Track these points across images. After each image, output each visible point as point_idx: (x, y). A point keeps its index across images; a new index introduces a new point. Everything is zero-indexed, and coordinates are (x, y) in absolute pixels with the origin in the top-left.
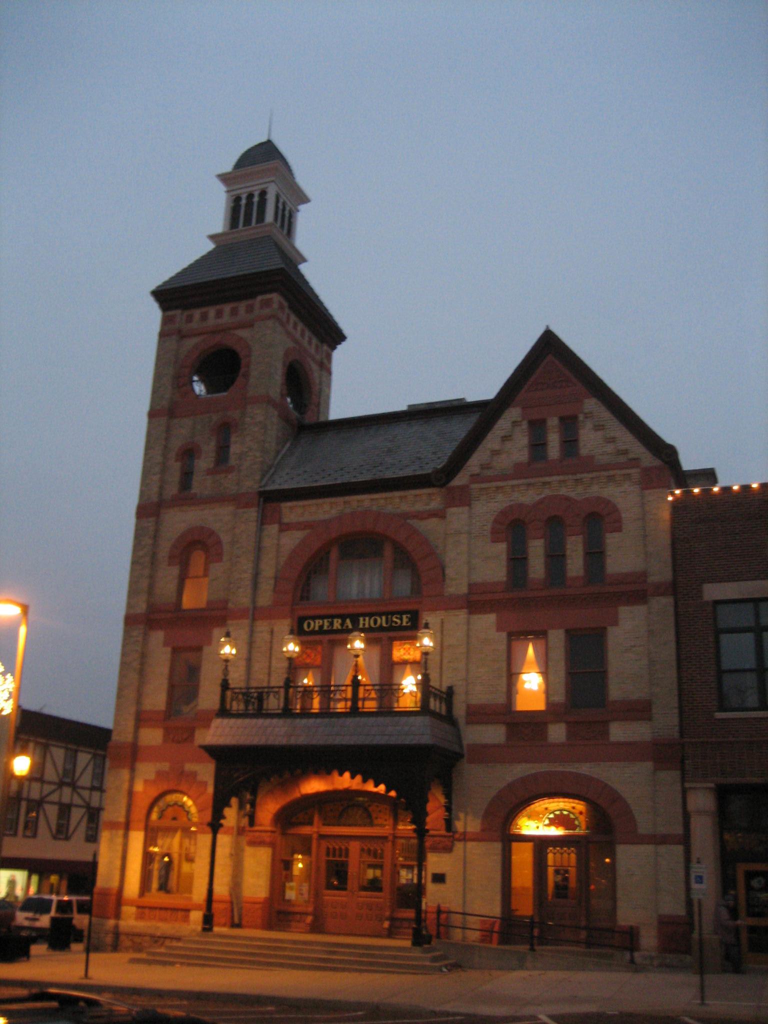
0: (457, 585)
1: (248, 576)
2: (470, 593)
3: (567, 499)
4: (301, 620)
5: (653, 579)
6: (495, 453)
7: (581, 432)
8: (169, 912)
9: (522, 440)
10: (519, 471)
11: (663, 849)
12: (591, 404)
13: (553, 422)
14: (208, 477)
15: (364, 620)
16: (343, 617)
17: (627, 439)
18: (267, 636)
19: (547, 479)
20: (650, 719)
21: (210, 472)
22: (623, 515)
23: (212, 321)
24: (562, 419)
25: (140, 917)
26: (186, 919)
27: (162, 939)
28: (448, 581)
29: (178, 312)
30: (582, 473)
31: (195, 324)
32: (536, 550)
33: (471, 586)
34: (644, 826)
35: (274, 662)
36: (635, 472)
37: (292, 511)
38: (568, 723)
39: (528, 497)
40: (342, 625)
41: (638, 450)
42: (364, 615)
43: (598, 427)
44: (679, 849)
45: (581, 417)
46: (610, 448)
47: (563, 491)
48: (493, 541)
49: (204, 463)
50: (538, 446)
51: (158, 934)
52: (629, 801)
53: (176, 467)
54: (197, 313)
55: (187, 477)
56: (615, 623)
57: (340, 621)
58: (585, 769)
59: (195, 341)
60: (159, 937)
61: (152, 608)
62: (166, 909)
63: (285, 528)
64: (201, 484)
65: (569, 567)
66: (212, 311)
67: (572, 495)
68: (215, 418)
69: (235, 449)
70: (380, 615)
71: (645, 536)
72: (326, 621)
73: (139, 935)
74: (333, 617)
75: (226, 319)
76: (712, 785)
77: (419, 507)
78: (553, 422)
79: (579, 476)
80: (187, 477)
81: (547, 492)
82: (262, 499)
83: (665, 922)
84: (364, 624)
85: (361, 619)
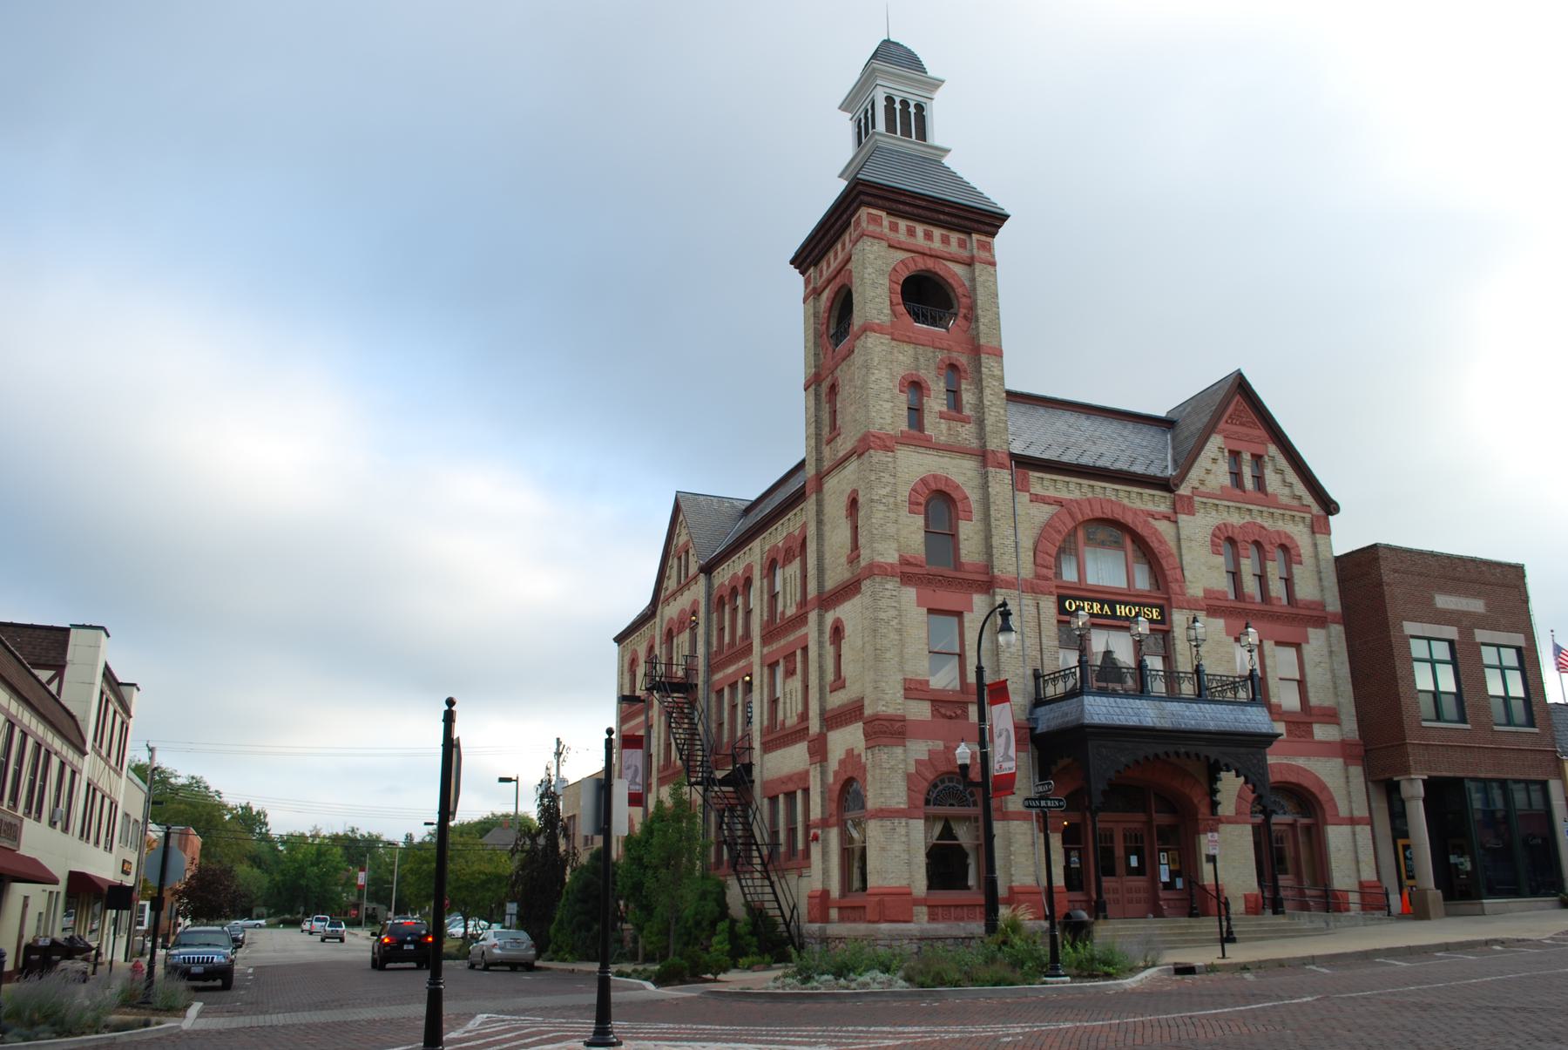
0: (1195, 589)
1: (1010, 542)
3: (1263, 527)
4: (1061, 600)
5: (1330, 609)
6: (1208, 471)
7: (1266, 471)
8: (965, 909)
9: (1223, 468)
10: (1223, 495)
11: (1358, 828)
12: (1273, 449)
13: (1246, 457)
14: (942, 421)
15: (1120, 608)
16: (1102, 602)
17: (1300, 488)
18: (1033, 611)
19: (1250, 507)
20: (1338, 724)
21: (942, 415)
22: (1302, 551)
23: (920, 240)
24: (1253, 455)
25: (933, 918)
27: (967, 940)
28: (1187, 583)
29: (883, 214)
30: (1274, 508)
31: (902, 236)
32: (1248, 566)
33: (1206, 591)
34: (1343, 811)
35: (1044, 640)
36: (1308, 516)
37: (1041, 483)
38: (1286, 722)
39: (1236, 519)
40: (1102, 609)
41: (1308, 499)
42: (1121, 603)
43: (1280, 472)
44: (1368, 828)
45: (1266, 458)
46: (1286, 491)
47: (1259, 520)
48: (1213, 553)
49: (936, 403)
50: (1237, 476)
51: (964, 936)
52: (1332, 789)
53: (903, 400)
54: (903, 224)
56: (1307, 642)
57: (1099, 606)
58: (1301, 762)
59: (901, 255)
60: (964, 938)
61: (904, 561)
62: (962, 906)
63: (1036, 498)
64: (936, 428)
65: (1271, 587)
66: (920, 229)
68: (940, 355)
69: (968, 397)
71: (1319, 572)
72: (1086, 603)
74: (1093, 600)
75: (937, 245)
76: (1426, 777)
77: (1150, 507)
78: (1246, 457)
79: (1271, 510)
81: (1248, 518)
82: (1013, 462)
83: (1363, 887)
84: (1121, 612)
85: (1118, 606)
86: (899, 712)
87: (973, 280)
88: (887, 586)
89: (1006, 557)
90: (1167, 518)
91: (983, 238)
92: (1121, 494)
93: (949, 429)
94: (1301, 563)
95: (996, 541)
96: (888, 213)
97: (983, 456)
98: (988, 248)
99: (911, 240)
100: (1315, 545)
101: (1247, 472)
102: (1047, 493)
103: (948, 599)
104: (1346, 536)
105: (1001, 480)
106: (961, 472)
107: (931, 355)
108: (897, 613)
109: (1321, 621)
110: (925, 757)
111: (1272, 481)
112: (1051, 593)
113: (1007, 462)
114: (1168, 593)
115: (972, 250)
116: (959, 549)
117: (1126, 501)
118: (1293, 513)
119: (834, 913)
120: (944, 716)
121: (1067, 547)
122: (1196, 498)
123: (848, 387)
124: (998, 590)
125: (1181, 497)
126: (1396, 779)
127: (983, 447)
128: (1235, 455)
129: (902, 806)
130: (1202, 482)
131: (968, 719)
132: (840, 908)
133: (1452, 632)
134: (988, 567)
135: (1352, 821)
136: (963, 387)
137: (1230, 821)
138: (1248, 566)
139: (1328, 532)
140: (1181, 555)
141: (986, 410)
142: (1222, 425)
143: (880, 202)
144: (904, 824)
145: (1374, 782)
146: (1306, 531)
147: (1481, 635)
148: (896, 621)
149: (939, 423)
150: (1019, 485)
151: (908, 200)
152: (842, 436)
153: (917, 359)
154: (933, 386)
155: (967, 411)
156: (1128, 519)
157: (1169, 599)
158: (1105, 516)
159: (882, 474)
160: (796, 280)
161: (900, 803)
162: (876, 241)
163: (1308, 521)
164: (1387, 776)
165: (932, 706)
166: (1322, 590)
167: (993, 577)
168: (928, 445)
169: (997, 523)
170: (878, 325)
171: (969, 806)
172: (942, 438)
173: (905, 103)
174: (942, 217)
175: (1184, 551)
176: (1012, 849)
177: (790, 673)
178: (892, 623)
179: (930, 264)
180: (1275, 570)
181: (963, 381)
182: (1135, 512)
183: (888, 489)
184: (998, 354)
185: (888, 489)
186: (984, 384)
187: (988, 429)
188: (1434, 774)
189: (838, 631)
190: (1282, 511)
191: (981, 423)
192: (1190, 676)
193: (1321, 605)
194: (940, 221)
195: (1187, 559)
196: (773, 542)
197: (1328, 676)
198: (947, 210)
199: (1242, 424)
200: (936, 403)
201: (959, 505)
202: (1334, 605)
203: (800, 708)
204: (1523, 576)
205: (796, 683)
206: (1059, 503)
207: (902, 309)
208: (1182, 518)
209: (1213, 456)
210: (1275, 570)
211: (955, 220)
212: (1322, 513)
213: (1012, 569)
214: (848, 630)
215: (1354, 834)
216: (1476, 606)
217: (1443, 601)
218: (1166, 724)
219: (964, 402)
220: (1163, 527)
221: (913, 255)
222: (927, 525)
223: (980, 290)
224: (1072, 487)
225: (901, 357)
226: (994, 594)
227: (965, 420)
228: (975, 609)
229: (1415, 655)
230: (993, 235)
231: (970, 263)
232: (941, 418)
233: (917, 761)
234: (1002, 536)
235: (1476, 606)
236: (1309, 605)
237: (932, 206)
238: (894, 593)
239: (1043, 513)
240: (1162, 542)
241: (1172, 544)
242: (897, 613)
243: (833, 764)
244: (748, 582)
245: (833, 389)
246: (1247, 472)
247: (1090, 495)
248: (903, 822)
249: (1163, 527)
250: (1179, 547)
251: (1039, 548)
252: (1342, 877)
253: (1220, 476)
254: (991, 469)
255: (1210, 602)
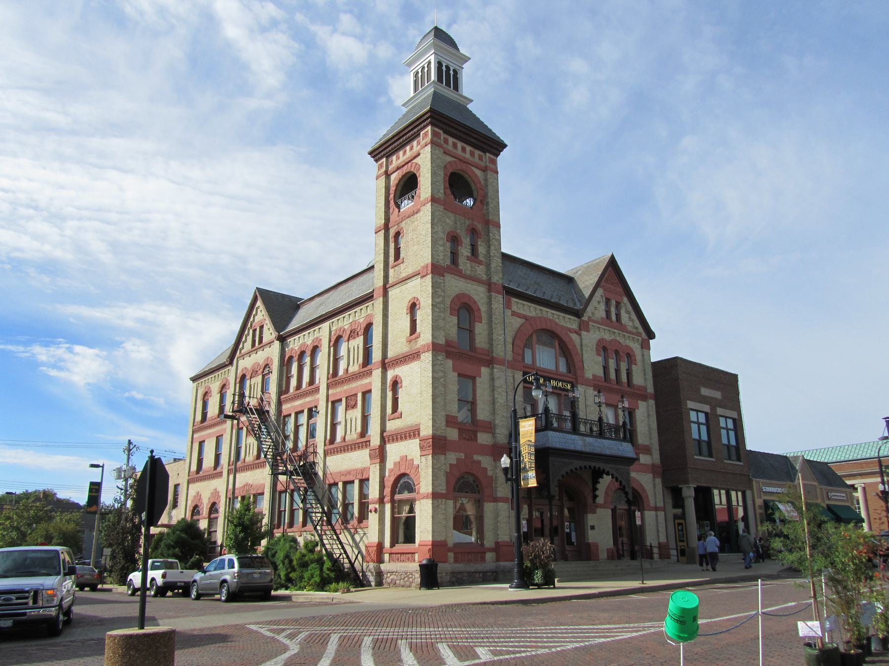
0: (589, 375)
2: (593, 379)
3: (620, 343)
5: (649, 391)
9: (602, 307)
11: (659, 513)
12: (625, 300)
13: (613, 302)
14: (468, 262)
17: (637, 324)
19: (615, 331)
24: (616, 302)
26: (483, 560)
29: (441, 132)
32: (612, 363)
33: (593, 376)
34: (652, 504)
37: (518, 305)
39: (608, 337)
41: (641, 330)
42: (554, 379)
43: (628, 312)
44: (663, 512)
45: (622, 304)
46: (631, 324)
47: (618, 338)
49: (465, 251)
50: (608, 312)
51: (473, 571)
54: (451, 140)
55: (454, 255)
56: (638, 408)
59: (449, 159)
60: (473, 572)
63: (514, 314)
64: (464, 265)
67: (621, 341)
69: (482, 250)
70: (560, 380)
73: (460, 573)
75: (467, 156)
76: (695, 486)
77: (568, 325)
78: (613, 302)
79: (624, 333)
80: (454, 255)
81: (613, 337)
83: (660, 546)
86: (443, 434)
87: (486, 180)
88: (440, 358)
89: (500, 347)
90: (576, 332)
91: (492, 156)
92: (555, 316)
93: (472, 267)
94: (636, 364)
95: (495, 336)
96: (444, 132)
97: (490, 286)
98: (494, 162)
99: (455, 151)
100: (643, 355)
101: (613, 310)
102: (519, 311)
103: (468, 368)
104: (659, 352)
105: (498, 300)
106: (478, 293)
107: (463, 221)
108: (443, 374)
109: (644, 398)
110: (455, 462)
111: (624, 317)
112: (520, 370)
113: (501, 289)
114: (575, 375)
115: (486, 162)
116: (475, 339)
117: (557, 320)
118: (634, 336)
119: (386, 557)
120: (465, 439)
121: (528, 344)
122: (590, 323)
123: (411, 234)
124: (495, 365)
125: (584, 321)
126: (680, 486)
127: (490, 279)
128: (608, 302)
129: (443, 492)
130: (593, 314)
131: (476, 440)
132: (390, 554)
133: (707, 408)
134: (490, 351)
135: (656, 509)
136: (479, 243)
137: (601, 506)
138: (612, 363)
139: (648, 348)
140: (582, 354)
141: (492, 258)
142: (603, 283)
143: (440, 125)
144: (444, 503)
145: (666, 488)
146: (639, 347)
147: (720, 411)
148: (443, 379)
149: (466, 263)
150: (508, 306)
151: (456, 126)
152: (404, 264)
153: (456, 223)
154: (464, 241)
155: (481, 258)
156: (558, 331)
157: (576, 379)
158: (547, 328)
159: (437, 290)
160: (372, 167)
161: (442, 490)
162: (437, 148)
163: (640, 341)
164: (675, 485)
165: (459, 431)
166: (645, 381)
167: (493, 358)
168: (460, 274)
169: (496, 326)
170: (437, 198)
171: (475, 493)
172: (468, 272)
173: (448, 67)
174: (472, 140)
175: (584, 352)
176: (499, 519)
177: (350, 406)
178: (441, 380)
179: (464, 166)
180: (624, 366)
181: (479, 240)
182: (563, 327)
183: (440, 299)
184: (498, 226)
185: (440, 299)
186: (491, 243)
187: (493, 270)
188: (699, 484)
189: (396, 384)
190: (628, 335)
191: (488, 266)
192: (596, 423)
193: (645, 388)
194: (470, 142)
195: (585, 357)
196: (340, 324)
197: (647, 428)
198: (475, 136)
199: (612, 284)
200: (465, 251)
201: (475, 313)
202: (650, 390)
203: (359, 429)
204: (737, 381)
205: (357, 413)
206: (525, 317)
207: (449, 191)
208: (584, 333)
209: (598, 300)
210: (624, 366)
211: (478, 143)
212: (646, 338)
213: (502, 354)
214: (405, 383)
215: (657, 516)
216: (717, 395)
217: (705, 391)
218: (587, 449)
219: (479, 252)
220: (574, 337)
221: (455, 159)
222: (458, 324)
223: (490, 187)
224: (532, 309)
225: (448, 221)
226: (493, 368)
227: (480, 263)
228: (482, 376)
229: (692, 419)
230: (497, 155)
231: (484, 170)
232: (468, 260)
233: (450, 465)
234: (498, 336)
235: (717, 395)
236: (640, 388)
237: (468, 132)
238: (442, 362)
239: (517, 322)
240: (574, 346)
241: (578, 347)
242: (443, 374)
243: (389, 465)
244: (315, 349)
245: (398, 234)
246: (613, 310)
247: (540, 315)
248: (444, 500)
249: (574, 337)
250: (582, 350)
251: (515, 343)
252: (651, 539)
253: (601, 313)
254: (493, 294)
255: (596, 382)
